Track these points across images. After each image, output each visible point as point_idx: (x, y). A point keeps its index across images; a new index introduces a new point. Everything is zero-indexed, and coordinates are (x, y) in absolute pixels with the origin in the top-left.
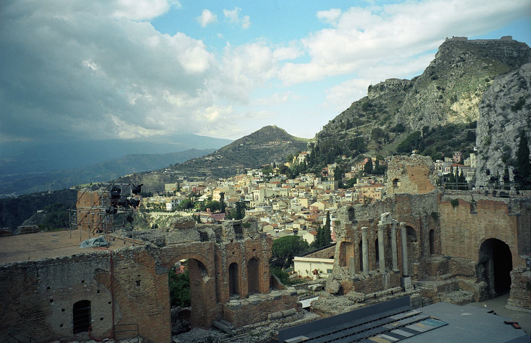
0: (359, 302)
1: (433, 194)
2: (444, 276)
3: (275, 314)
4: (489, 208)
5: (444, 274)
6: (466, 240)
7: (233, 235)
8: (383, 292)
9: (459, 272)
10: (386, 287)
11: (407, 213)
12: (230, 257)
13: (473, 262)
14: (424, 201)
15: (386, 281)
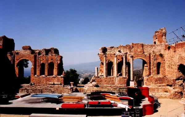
0: (94, 86)
1: (161, 45)
2: (159, 85)
3: (50, 83)
4: (180, 48)
5: (160, 83)
6: (173, 67)
7: (44, 53)
8: (113, 85)
9: (168, 83)
10: (116, 84)
11: (140, 52)
12: (42, 60)
13: (174, 78)
14: (154, 48)
15: (117, 81)
